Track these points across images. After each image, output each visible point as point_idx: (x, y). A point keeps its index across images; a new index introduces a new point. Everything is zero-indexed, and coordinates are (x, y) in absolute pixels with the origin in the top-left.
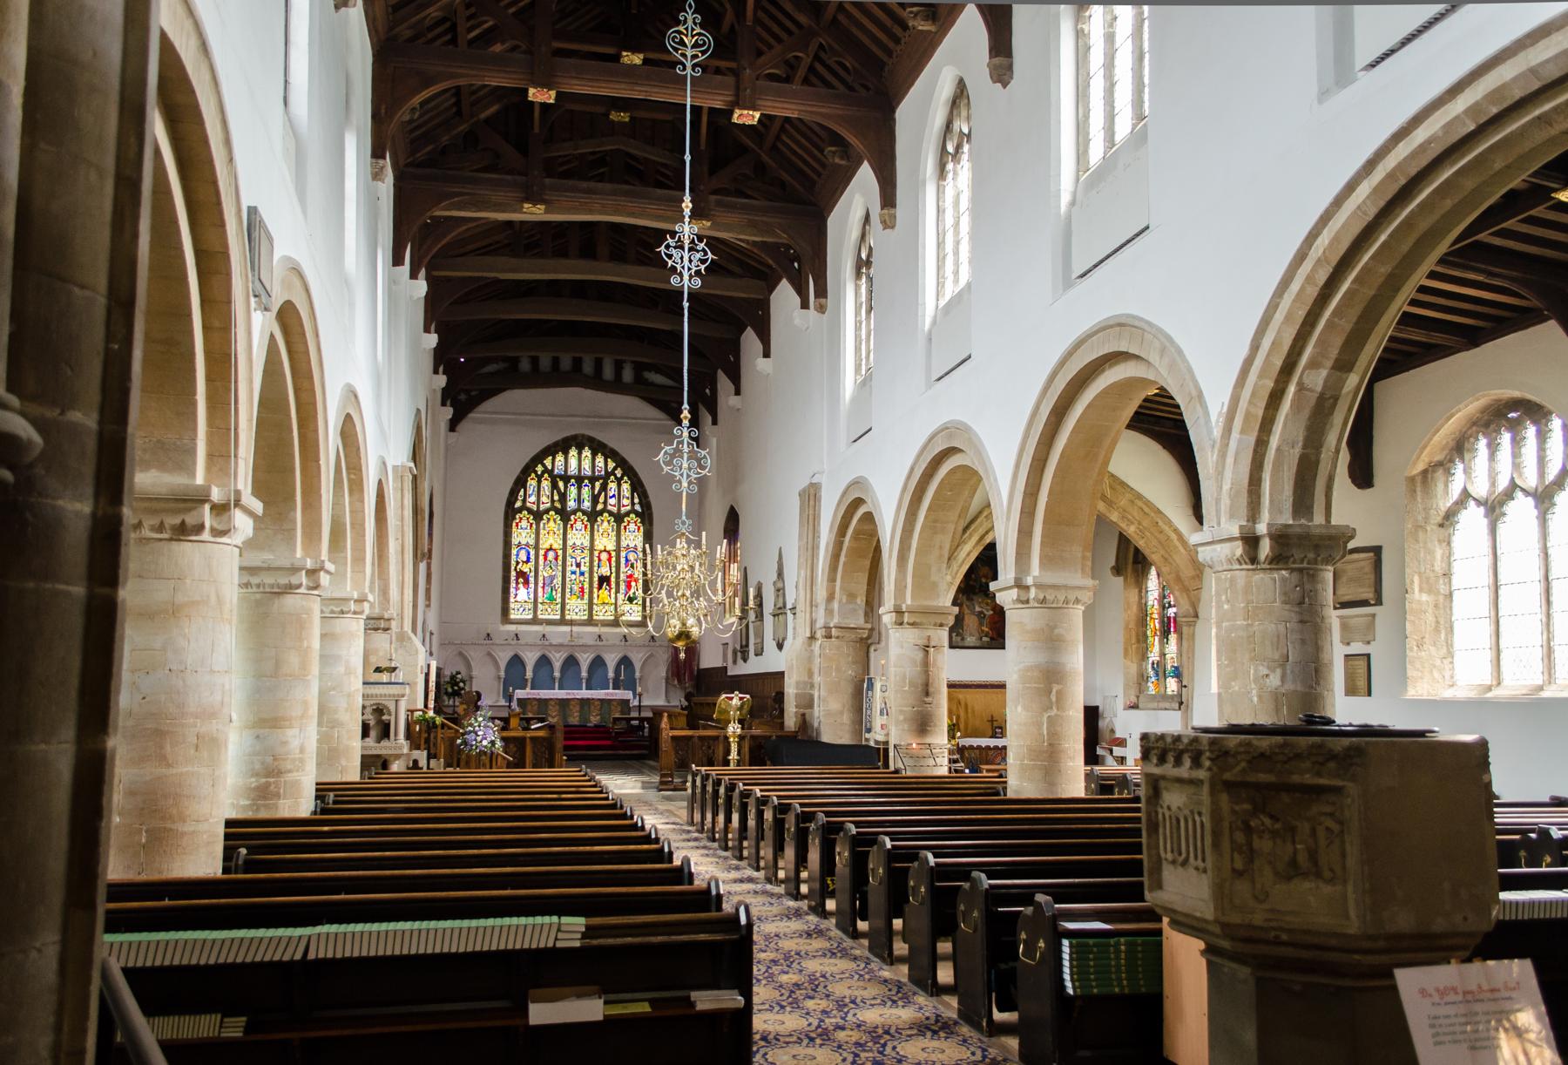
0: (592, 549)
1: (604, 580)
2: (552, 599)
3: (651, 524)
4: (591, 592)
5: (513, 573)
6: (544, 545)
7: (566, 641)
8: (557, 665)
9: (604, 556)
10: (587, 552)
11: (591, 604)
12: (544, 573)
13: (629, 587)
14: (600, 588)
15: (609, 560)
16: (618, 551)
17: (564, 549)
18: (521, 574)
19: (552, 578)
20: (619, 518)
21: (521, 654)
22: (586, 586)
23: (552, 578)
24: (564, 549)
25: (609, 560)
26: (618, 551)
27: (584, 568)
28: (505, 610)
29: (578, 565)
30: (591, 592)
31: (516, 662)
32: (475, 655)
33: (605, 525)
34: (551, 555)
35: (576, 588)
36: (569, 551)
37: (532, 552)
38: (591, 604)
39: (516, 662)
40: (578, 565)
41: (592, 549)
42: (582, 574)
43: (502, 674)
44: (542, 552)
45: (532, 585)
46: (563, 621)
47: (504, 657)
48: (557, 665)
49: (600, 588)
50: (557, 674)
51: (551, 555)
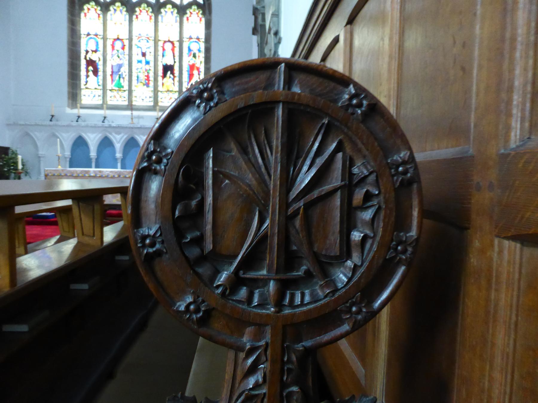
0: (156, 41)
1: (168, 69)
2: (120, 87)
3: (210, 13)
4: (156, 80)
5: (83, 63)
6: (111, 35)
7: (125, 123)
8: (118, 146)
9: (168, 46)
10: (152, 43)
11: (156, 91)
12: (112, 61)
13: (191, 76)
14: (164, 76)
15: (173, 50)
16: (181, 42)
17: (130, 39)
18: (90, 62)
19: (120, 66)
20: (182, 10)
21: (84, 135)
22: (151, 75)
23: (120, 66)
24: (130, 39)
25: (173, 50)
26: (181, 42)
27: (150, 57)
28: (74, 95)
29: (144, 55)
30: (156, 80)
31: (80, 143)
32: (39, 136)
33: (169, 15)
34: (118, 44)
35: (143, 77)
36: (135, 41)
37: (101, 42)
38: (156, 91)
39: (80, 143)
40: (144, 55)
41: (156, 41)
42: (148, 63)
43: (68, 153)
44: (109, 43)
45: (100, 73)
46: (130, 107)
47: (67, 139)
48: (118, 146)
49: (164, 76)
50: (119, 155)
51: (118, 44)
